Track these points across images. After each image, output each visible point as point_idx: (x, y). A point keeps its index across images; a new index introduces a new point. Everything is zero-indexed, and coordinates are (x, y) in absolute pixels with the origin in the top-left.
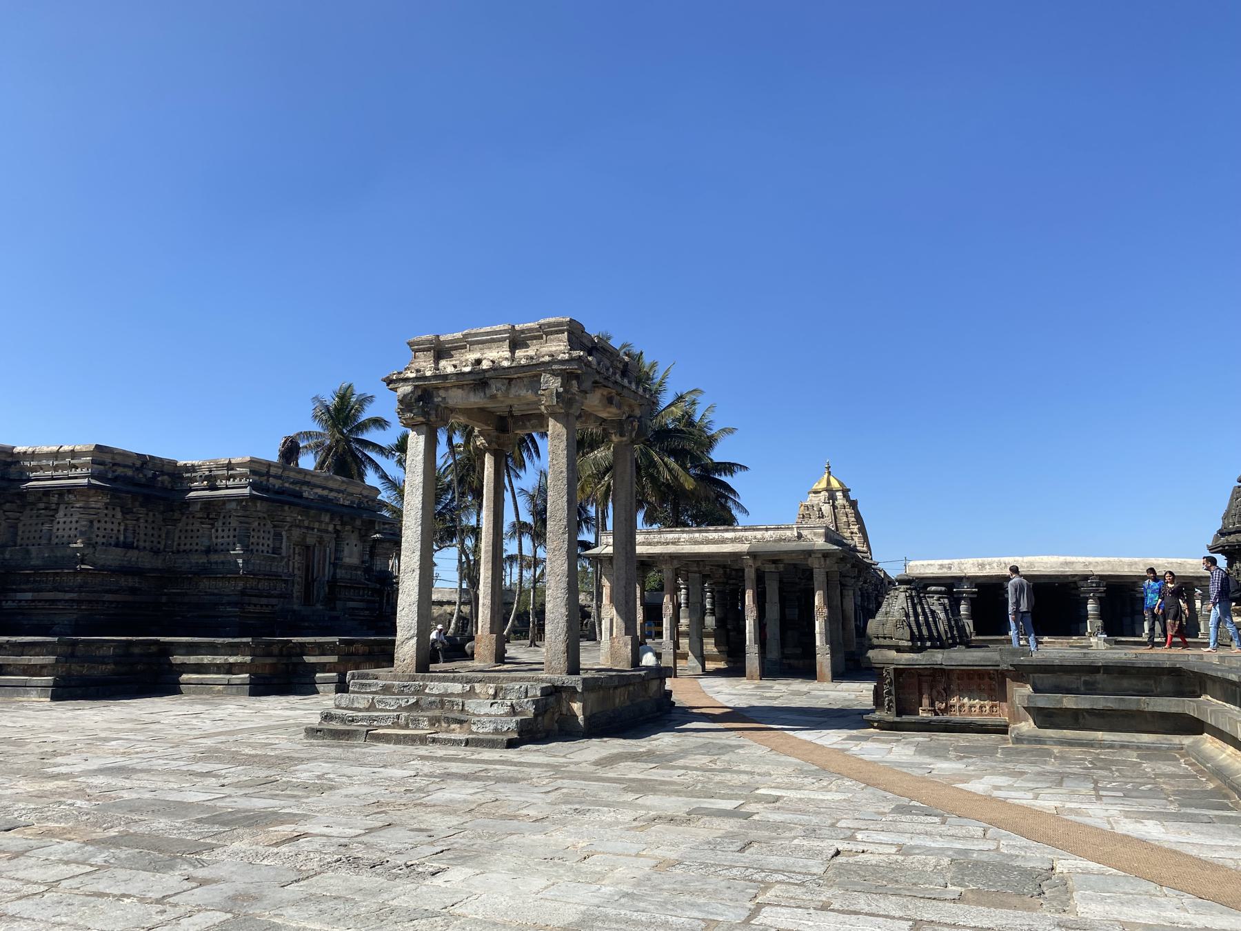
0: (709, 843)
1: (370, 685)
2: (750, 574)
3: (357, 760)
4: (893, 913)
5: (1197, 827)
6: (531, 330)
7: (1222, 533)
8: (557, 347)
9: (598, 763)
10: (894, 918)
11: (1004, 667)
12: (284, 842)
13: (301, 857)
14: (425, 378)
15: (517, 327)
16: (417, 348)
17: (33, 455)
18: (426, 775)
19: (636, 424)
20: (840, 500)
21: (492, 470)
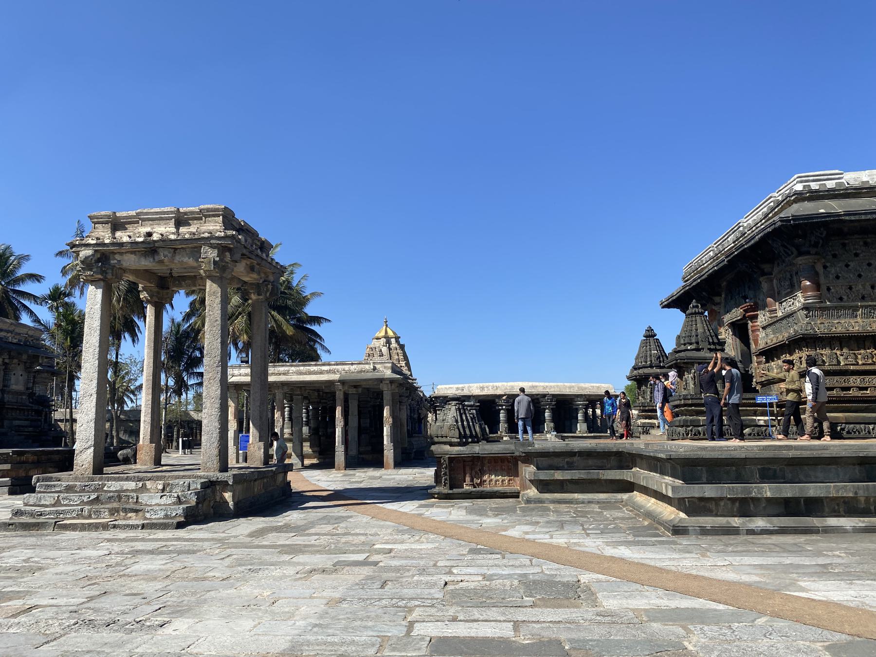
0: (357, 584)
2: (339, 395)
3: (53, 545)
4: (498, 618)
5: (649, 548)
6: (192, 213)
7: (635, 368)
8: (214, 227)
9: (251, 535)
10: (500, 621)
11: (517, 454)
12: (19, 614)
13: (42, 624)
14: (105, 245)
16: (96, 221)
18: (118, 553)
19: (270, 287)
20: (394, 344)
21: (153, 318)
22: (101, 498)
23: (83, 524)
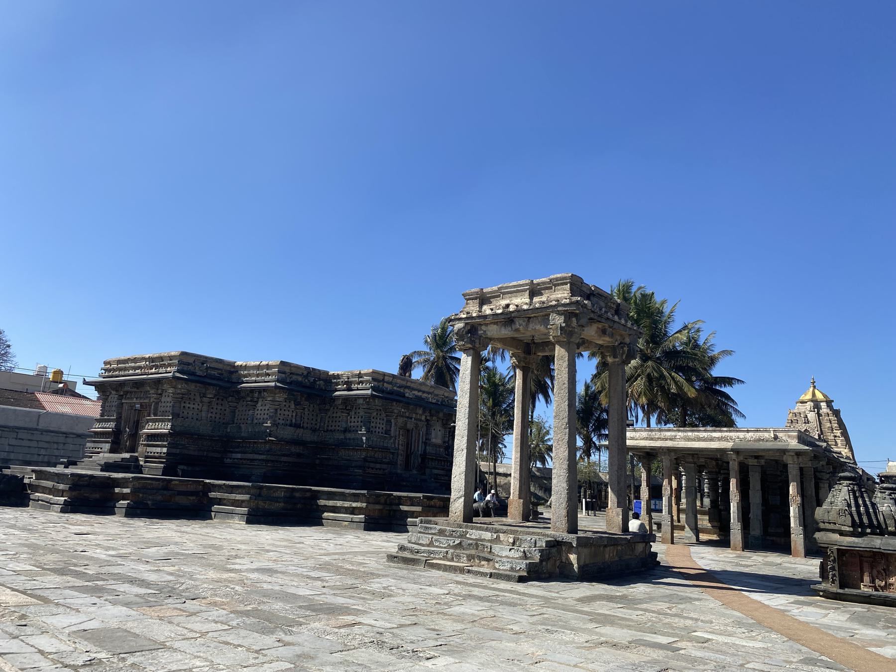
0: (634, 665)
1: (431, 528)
2: (734, 466)
3: (414, 579)
6: (544, 283)
8: (563, 294)
9: (580, 600)
12: (344, 626)
13: (350, 637)
14: (472, 318)
15: (535, 282)
16: (468, 297)
17: (246, 367)
18: (455, 595)
19: (626, 349)
20: (824, 409)
21: (521, 381)
22: (463, 544)
23: (445, 565)
